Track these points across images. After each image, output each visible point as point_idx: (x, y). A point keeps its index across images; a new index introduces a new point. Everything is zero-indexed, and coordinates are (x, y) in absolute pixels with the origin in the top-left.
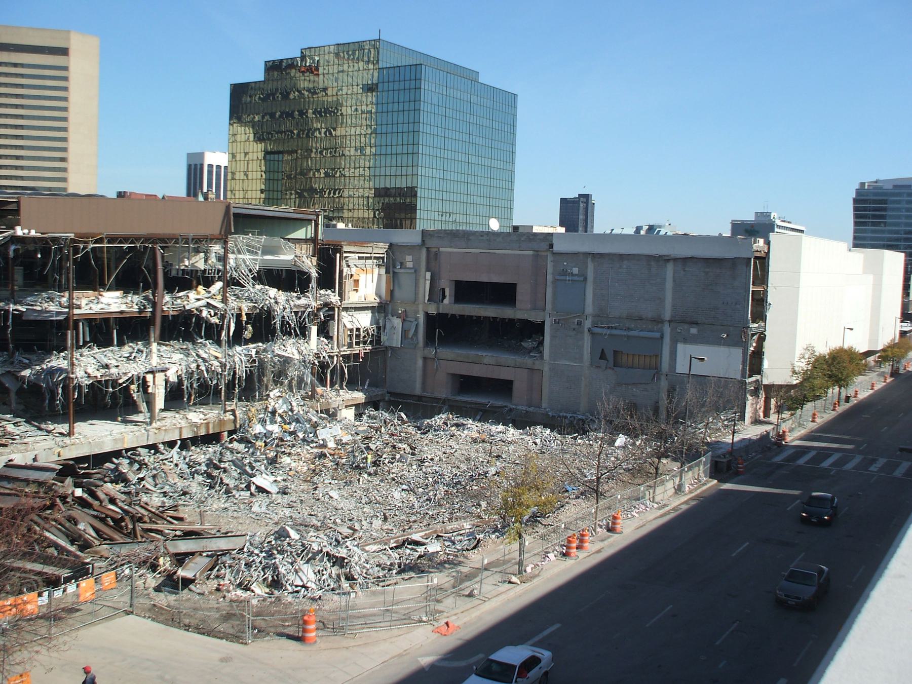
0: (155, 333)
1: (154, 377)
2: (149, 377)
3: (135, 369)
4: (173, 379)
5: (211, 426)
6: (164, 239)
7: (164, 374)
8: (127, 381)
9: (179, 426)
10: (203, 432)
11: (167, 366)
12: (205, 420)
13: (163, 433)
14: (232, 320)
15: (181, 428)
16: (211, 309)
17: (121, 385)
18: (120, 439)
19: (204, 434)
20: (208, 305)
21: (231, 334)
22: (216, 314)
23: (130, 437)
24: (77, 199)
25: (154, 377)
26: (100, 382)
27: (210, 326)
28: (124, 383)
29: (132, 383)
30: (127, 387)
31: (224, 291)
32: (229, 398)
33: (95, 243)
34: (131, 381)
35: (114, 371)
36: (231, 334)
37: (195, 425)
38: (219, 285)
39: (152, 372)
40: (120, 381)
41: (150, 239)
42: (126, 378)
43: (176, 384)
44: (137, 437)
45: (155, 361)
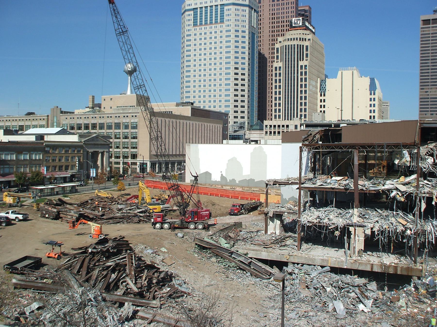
0: (356, 202)
1: (355, 230)
2: (352, 229)
3: (340, 222)
4: (368, 232)
5: (399, 269)
6: (364, 146)
7: (363, 228)
8: (334, 228)
9: (371, 263)
10: (391, 271)
11: (366, 224)
12: (397, 264)
13: (358, 264)
14: (422, 200)
15: (372, 264)
16: (399, 191)
17: (329, 229)
18: (326, 260)
19: (392, 273)
20: (397, 189)
21: (422, 210)
22: (403, 195)
23: (333, 260)
24: (356, 126)
25: (355, 230)
26: (316, 225)
27: (399, 202)
28: (332, 229)
29: (337, 230)
30: (333, 232)
31: (417, 179)
32: (420, 254)
33: (315, 149)
34: (336, 228)
35: (326, 221)
36: (422, 210)
37: (385, 265)
38: (414, 176)
39: (352, 226)
40: (330, 228)
41: (353, 146)
42: (333, 226)
43: (370, 236)
44: (338, 262)
45: (356, 219)
